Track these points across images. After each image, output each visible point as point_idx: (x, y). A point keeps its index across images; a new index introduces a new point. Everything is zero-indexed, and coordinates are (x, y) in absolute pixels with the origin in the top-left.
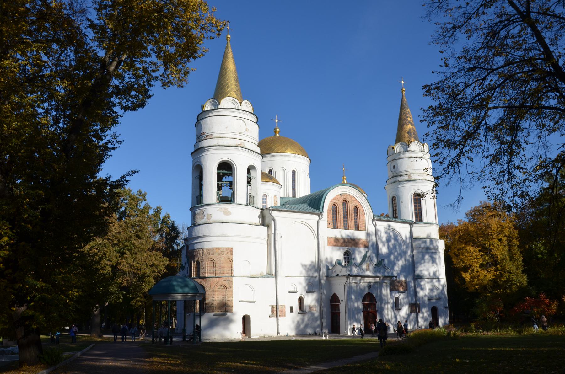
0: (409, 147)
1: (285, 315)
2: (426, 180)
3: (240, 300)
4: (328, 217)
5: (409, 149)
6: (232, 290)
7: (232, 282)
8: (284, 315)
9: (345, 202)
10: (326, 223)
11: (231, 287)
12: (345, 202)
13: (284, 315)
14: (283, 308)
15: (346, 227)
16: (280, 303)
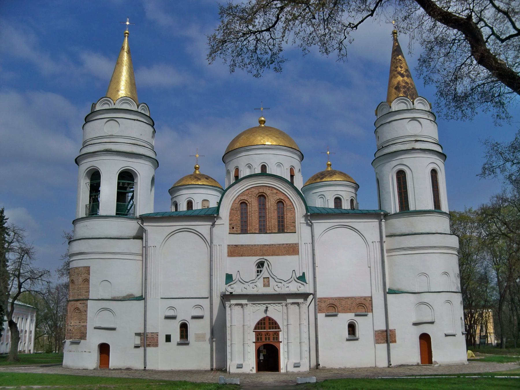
0: (390, 107)
1: (158, 345)
2: (413, 149)
3: (97, 325)
4: (230, 220)
5: (390, 111)
6: (86, 315)
7: (87, 305)
8: (156, 345)
9: (262, 197)
10: (227, 227)
11: (85, 311)
12: (262, 197)
13: (156, 345)
14: (155, 336)
15: (263, 230)
16: (149, 330)
